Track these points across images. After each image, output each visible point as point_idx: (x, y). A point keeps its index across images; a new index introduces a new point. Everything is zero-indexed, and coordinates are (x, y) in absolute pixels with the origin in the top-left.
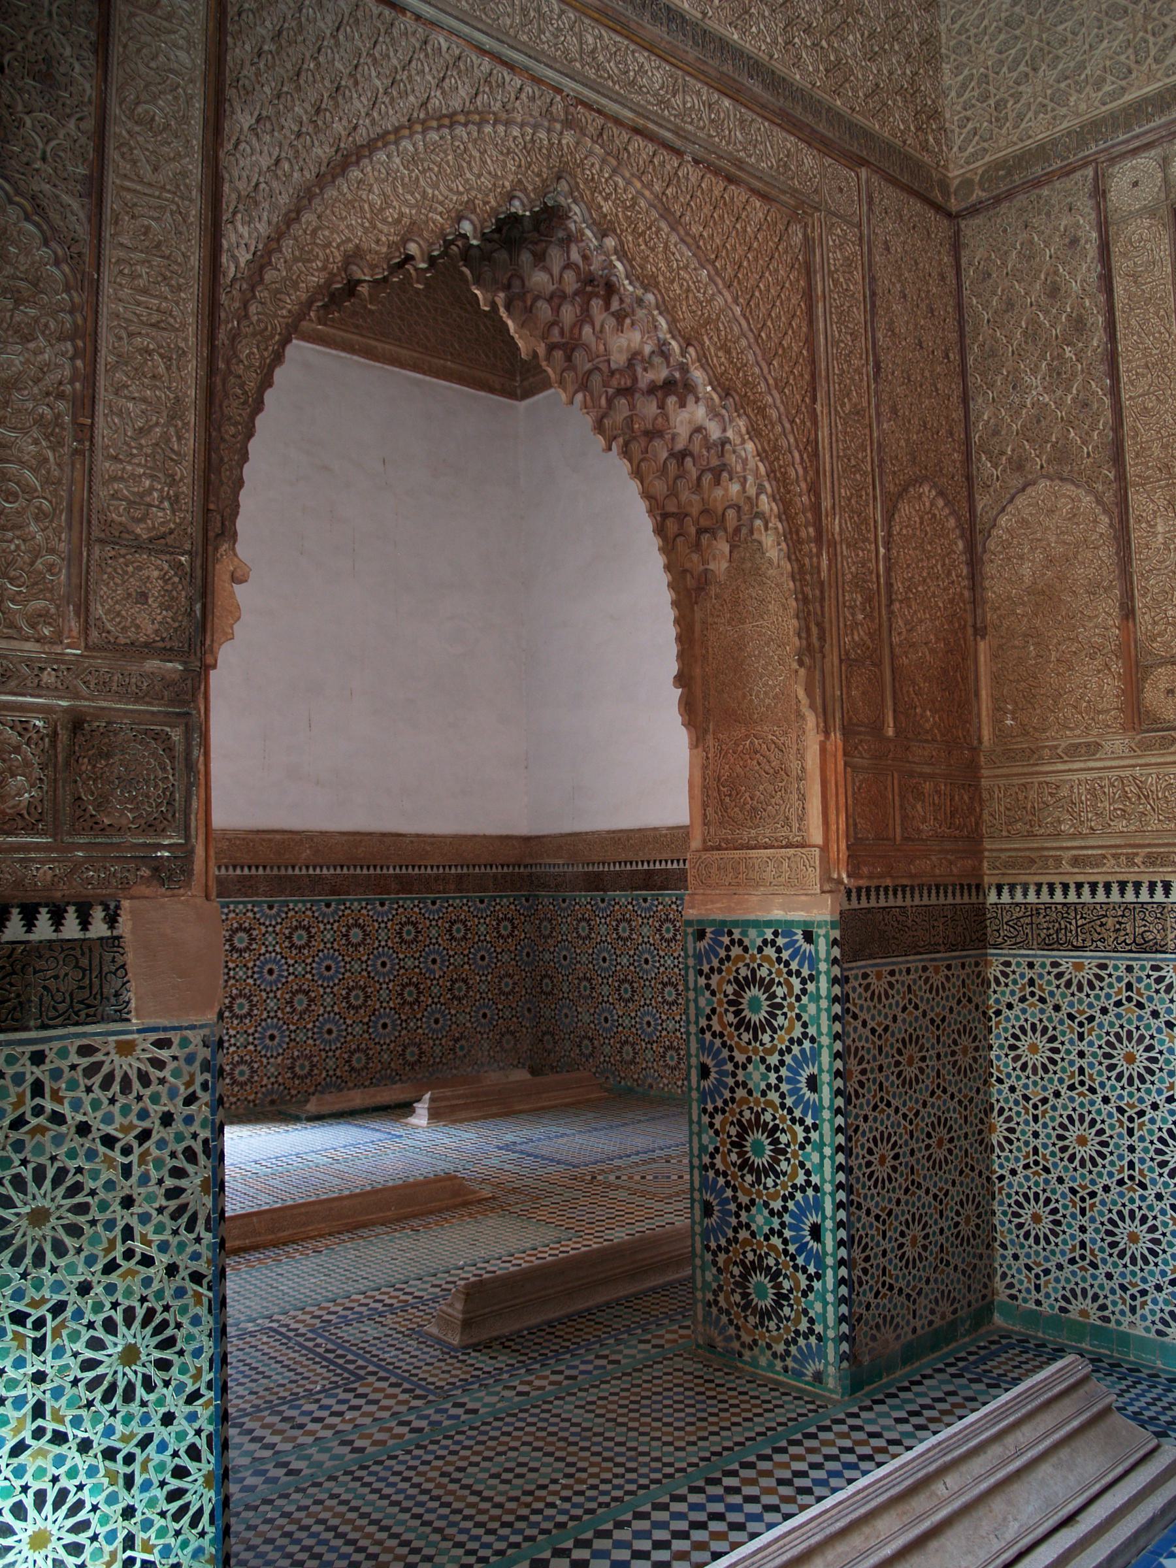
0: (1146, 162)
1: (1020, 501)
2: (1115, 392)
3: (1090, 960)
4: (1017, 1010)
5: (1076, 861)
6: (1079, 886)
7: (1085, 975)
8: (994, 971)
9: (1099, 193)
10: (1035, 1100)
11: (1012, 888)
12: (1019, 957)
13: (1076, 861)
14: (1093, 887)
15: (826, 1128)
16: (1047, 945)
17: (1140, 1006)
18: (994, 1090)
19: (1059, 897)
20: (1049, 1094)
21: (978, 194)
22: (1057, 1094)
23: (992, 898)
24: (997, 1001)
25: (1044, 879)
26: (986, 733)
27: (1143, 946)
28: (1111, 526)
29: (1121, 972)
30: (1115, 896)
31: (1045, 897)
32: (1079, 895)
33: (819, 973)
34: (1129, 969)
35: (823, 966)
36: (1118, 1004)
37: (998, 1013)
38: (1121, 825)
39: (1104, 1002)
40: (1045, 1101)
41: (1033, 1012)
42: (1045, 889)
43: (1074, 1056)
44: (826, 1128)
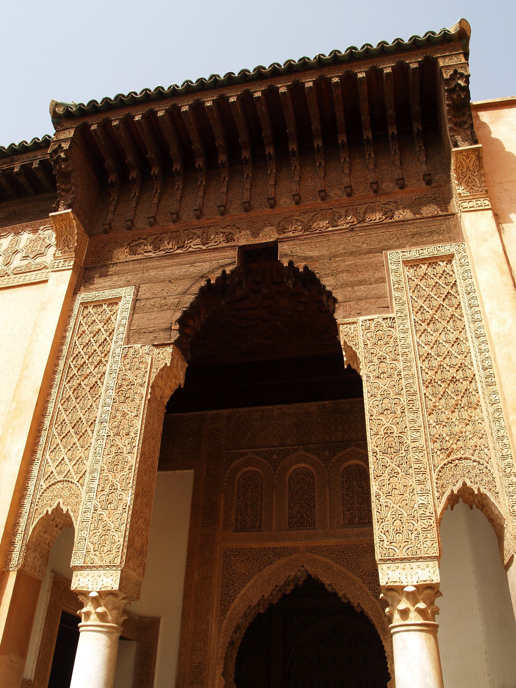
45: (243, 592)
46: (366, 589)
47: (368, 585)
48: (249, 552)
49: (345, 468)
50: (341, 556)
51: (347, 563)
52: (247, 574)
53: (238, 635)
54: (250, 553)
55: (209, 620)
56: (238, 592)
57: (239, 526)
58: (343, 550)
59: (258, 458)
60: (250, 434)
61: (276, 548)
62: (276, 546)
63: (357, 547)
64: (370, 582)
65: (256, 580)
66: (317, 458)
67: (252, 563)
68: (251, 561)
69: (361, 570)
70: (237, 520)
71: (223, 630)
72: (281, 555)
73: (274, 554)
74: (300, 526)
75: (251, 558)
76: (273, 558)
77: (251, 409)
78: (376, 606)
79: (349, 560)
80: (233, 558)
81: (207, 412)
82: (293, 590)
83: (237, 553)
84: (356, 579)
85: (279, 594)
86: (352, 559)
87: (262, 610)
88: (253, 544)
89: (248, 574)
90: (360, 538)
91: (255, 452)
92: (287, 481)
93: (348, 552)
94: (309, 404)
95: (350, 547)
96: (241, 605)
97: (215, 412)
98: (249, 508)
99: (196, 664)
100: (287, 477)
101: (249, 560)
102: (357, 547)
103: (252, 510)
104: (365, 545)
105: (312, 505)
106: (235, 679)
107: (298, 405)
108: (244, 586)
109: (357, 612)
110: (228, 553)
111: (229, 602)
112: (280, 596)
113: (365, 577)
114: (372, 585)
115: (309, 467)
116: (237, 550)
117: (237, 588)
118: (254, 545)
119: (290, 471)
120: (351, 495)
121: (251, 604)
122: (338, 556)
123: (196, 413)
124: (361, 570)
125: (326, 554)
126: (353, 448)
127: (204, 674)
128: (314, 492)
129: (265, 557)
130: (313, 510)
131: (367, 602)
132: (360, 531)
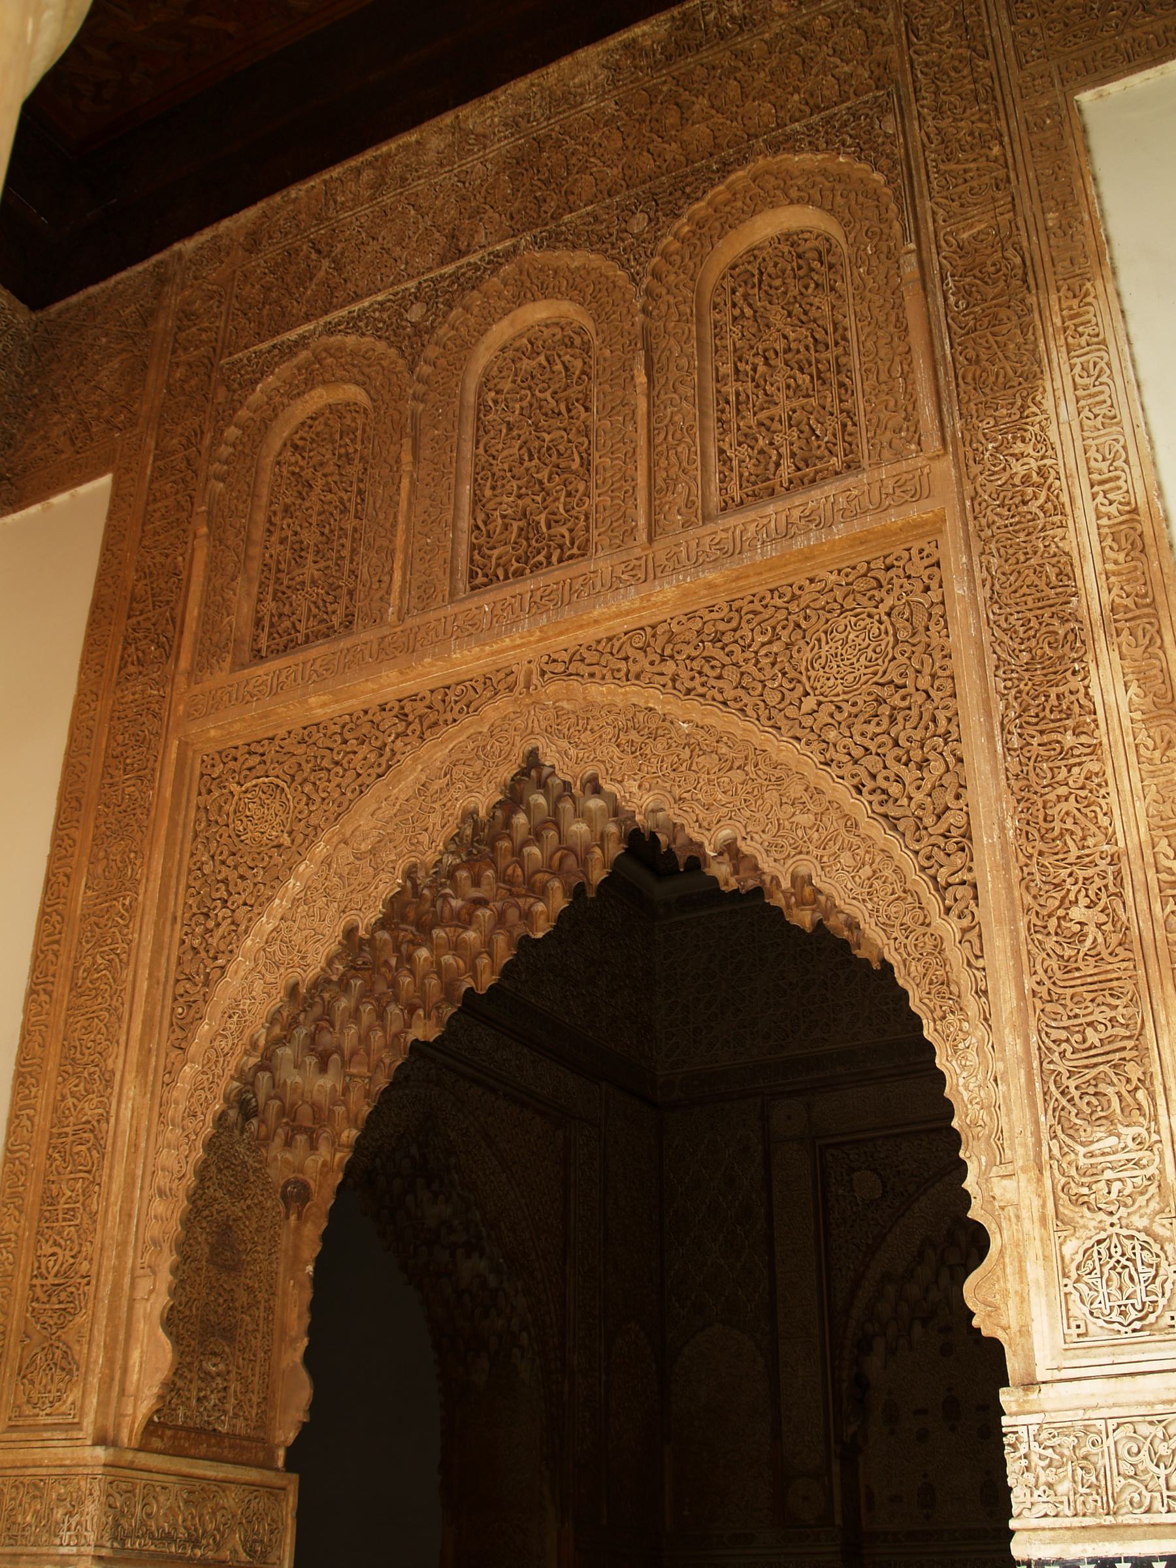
45: (266, 924)
46: (842, 792)
47: (849, 768)
48: (302, 741)
50: (707, 659)
52: (286, 840)
53: (324, 1152)
54: (301, 749)
55: (113, 1072)
58: (722, 626)
59: (351, 340)
61: (413, 698)
62: (410, 686)
63: (794, 597)
64: (857, 752)
65: (327, 862)
66: (595, 260)
67: (308, 788)
69: (809, 703)
70: (258, 622)
71: (175, 1112)
73: (401, 727)
75: (307, 767)
77: (336, 172)
78: (897, 870)
79: (750, 667)
81: (177, 247)
82: (563, 916)
83: (254, 761)
84: (783, 749)
85: (501, 941)
86: (765, 661)
87: (425, 1030)
88: (313, 700)
89: (286, 840)
90: (800, 543)
91: (339, 324)
93: (745, 631)
94: (565, 62)
95: (757, 606)
96: (258, 985)
97: (206, 235)
98: (311, 558)
99: (51, 1280)
101: (298, 779)
102: (794, 597)
103: (322, 564)
104: (834, 577)
106: (309, 1359)
107: (520, 86)
108: (270, 899)
111: (206, 983)
112: (504, 952)
113: (832, 735)
115: (566, 309)
117: (241, 912)
118: (320, 706)
119: (483, 356)
120: (761, 368)
121: (296, 975)
122: (696, 665)
123: (139, 268)
124: (809, 703)
125: (635, 669)
126: (761, 161)
127: (79, 1319)
129: (364, 750)
131: (846, 858)
132: (796, 513)
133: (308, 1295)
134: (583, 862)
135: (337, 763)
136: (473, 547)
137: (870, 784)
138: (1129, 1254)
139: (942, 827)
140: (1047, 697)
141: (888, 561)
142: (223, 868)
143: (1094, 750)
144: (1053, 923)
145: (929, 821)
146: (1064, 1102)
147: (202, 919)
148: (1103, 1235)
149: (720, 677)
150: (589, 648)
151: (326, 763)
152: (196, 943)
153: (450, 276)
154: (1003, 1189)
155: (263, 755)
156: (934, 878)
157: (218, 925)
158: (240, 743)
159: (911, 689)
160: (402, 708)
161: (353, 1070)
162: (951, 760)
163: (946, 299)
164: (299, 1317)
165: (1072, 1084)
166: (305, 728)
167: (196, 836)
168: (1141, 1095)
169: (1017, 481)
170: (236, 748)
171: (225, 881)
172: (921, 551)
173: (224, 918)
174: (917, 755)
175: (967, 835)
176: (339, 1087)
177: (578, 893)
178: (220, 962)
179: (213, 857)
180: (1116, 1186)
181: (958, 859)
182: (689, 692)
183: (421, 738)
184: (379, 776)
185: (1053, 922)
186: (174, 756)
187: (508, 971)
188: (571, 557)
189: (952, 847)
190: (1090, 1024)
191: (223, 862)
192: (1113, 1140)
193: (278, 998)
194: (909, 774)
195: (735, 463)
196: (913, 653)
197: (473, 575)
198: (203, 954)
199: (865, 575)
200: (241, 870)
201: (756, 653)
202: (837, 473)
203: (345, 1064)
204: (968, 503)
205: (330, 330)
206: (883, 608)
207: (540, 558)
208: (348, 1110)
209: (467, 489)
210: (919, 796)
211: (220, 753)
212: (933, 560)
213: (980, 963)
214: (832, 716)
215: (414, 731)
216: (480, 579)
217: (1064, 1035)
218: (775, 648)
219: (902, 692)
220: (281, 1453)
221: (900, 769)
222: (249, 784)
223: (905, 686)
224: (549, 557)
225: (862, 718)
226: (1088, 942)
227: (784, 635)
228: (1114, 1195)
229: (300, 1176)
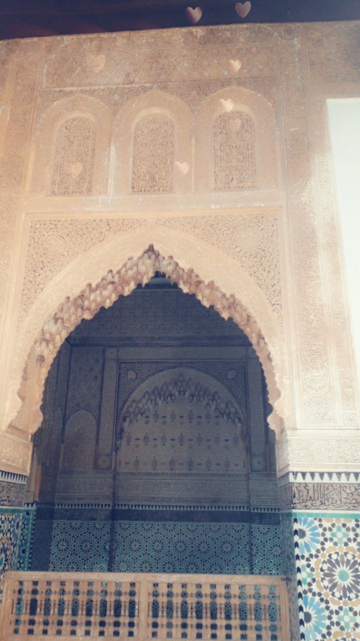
0: (113, 350)
1: (77, 413)
2: (101, 394)
3: (79, 523)
4: (59, 536)
5: (78, 499)
6: (79, 505)
7: (78, 526)
8: (55, 526)
9: (104, 352)
10: (62, 559)
11: (62, 505)
12: (61, 522)
13: (78, 499)
14: (82, 505)
15: (26, 563)
16: (69, 519)
17: (90, 533)
18: (51, 557)
19: (73, 507)
20: (66, 557)
21: (77, 342)
22: (68, 557)
23: (56, 507)
24: (55, 533)
25: (70, 503)
26: (61, 466)
27: (92, 519)
28: (96, 423)
29: (86, 525)
30: (87, 507)
31: (70, 507)
32: (78, 507)
33: (29, 523)
34: (88, 525)
35: (31, 521)
36: (85, 533)
37: (54, 537)
38: (90, 491)
39: (81, 533)
40: (64, 559)
41: (63, 536)
42: (70, 505)
43: (73, 547)
44: (26, 563)
48: (71, 224)
49: (220, 116)
50: (209, 231)
51: (217, 240)
52: (65, 253)
53: (51, 347)
54: (70, 227)
56: (51, 279)
57: (56, 190)
60: (79, 68)
67: (73, 239)
68: (72, 237)
69: (238, 249)
70: (53, 182)
72: (120, 230)
74: (149, 191)
75: (73, 233)
76: (107, 232)
80: (45, 233)
83: (53, 226)
87: (88, 316)
89: (65, 253)
92: (133, 131)
100: (133, 126)
105: (168, 162)
108: (60, 271)
109: (223, 319)
110: (37, 226)
112: (114, 298)
113: (244, 259)
114: (255, 269)
116: (52, 222)
119: (137, 119)
120: (228, 150)
124: (238, 249)
128: (173, 146)
130: (170, 171)
133: (43, 389)
134: (142, 277)
135: (84, 234)
136: (133, 179)
137: (254, 275)
138: (321, 401)
139: (273, 289)
140: (307, 262)
141: (263, 215)
142: (41, 258)
143: (318, 277)
144: (305, 318)
145: (270, 287)
146: (306, 362)
147: (33, 272)
148: (315, 396)
149: (211, 236)
150: (172, 219)
151: (80, 233)
152: (31, 279)
153: (128, 89)
154: (286, 382)
155: (56, 225)
156: (270, 302)
157: (40, 275)
158: (46, 219)
159: (266, 252)
160: (108, 222)
161: (66, 325)
162: (277, 273)
163: (286, 147)
164: (40, 395)
165: (308, 358)
166: (72, 220)
167: (29, 246)
168: (325, 363)
169: (303, 203)
170: (45, 221)
171: (42, 262)
172: (272, 215)
173: (42, 274)
174: (267, 269)
175: (280, 292)
176: (60, 329)
177: (139, 286)
178: (41, 286)
179: (37, 254)
180: (318, 385)
181: (277, 298)
182: (202, 239)
183: (115, 233)
184: (100, 241)
185: (305, 318)
186: (23, 218)
187: (115, 303)
188: (166, 191)
189: (276, 294)
190: (313, 345)
191: (41, 256)
192: (317, 374)
193: (63, 299)
194: (265, 274)
195: (219, 176)
196: (268, 242)
197: (133, 188)
198: (34, 283)
199: (256, 217)
200: (48, 259)
201: (223, 232)
202: (249, 187)
203: (63, 322)
204: (289, 205)
205: (82, 91)
206: (261, 228)
207: (156, 188)
208: (61, 337)
209: (131, 160)
210: (267, 280)
211: (39, 221)
212: (275, 218)
213: (282, 325)
214: (244, 254)
215: (112, 230)
216: (136, 189)
217: (306, 346)
218: (229, 232)
219: (264, 252)
220: (30, 436)
221: (264, 273)
222: (50, 234)
223: (264, 251)
224: (159, 189)
225: (252, 257)
226: (314, 325)
227: (231, 229)
228: (317, 387)
229: (42, 354)
